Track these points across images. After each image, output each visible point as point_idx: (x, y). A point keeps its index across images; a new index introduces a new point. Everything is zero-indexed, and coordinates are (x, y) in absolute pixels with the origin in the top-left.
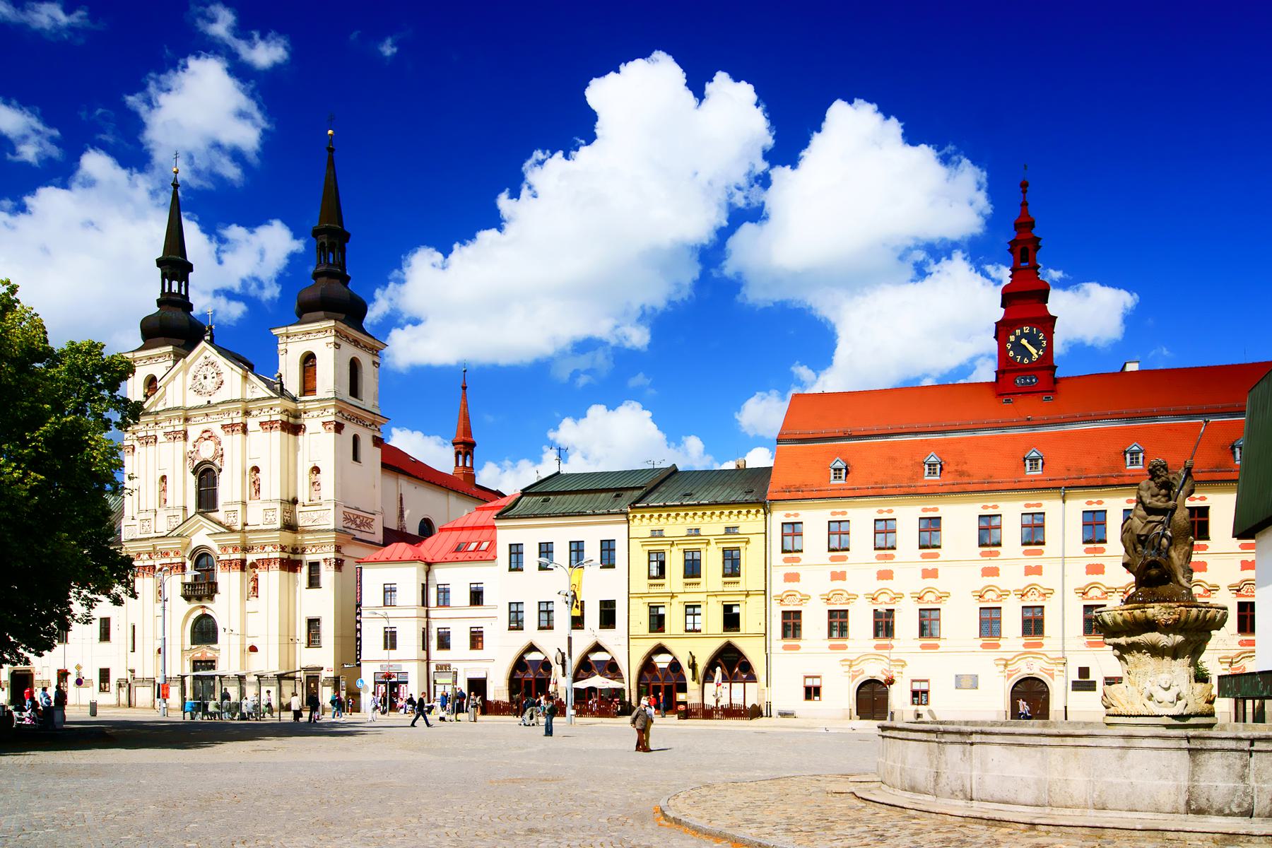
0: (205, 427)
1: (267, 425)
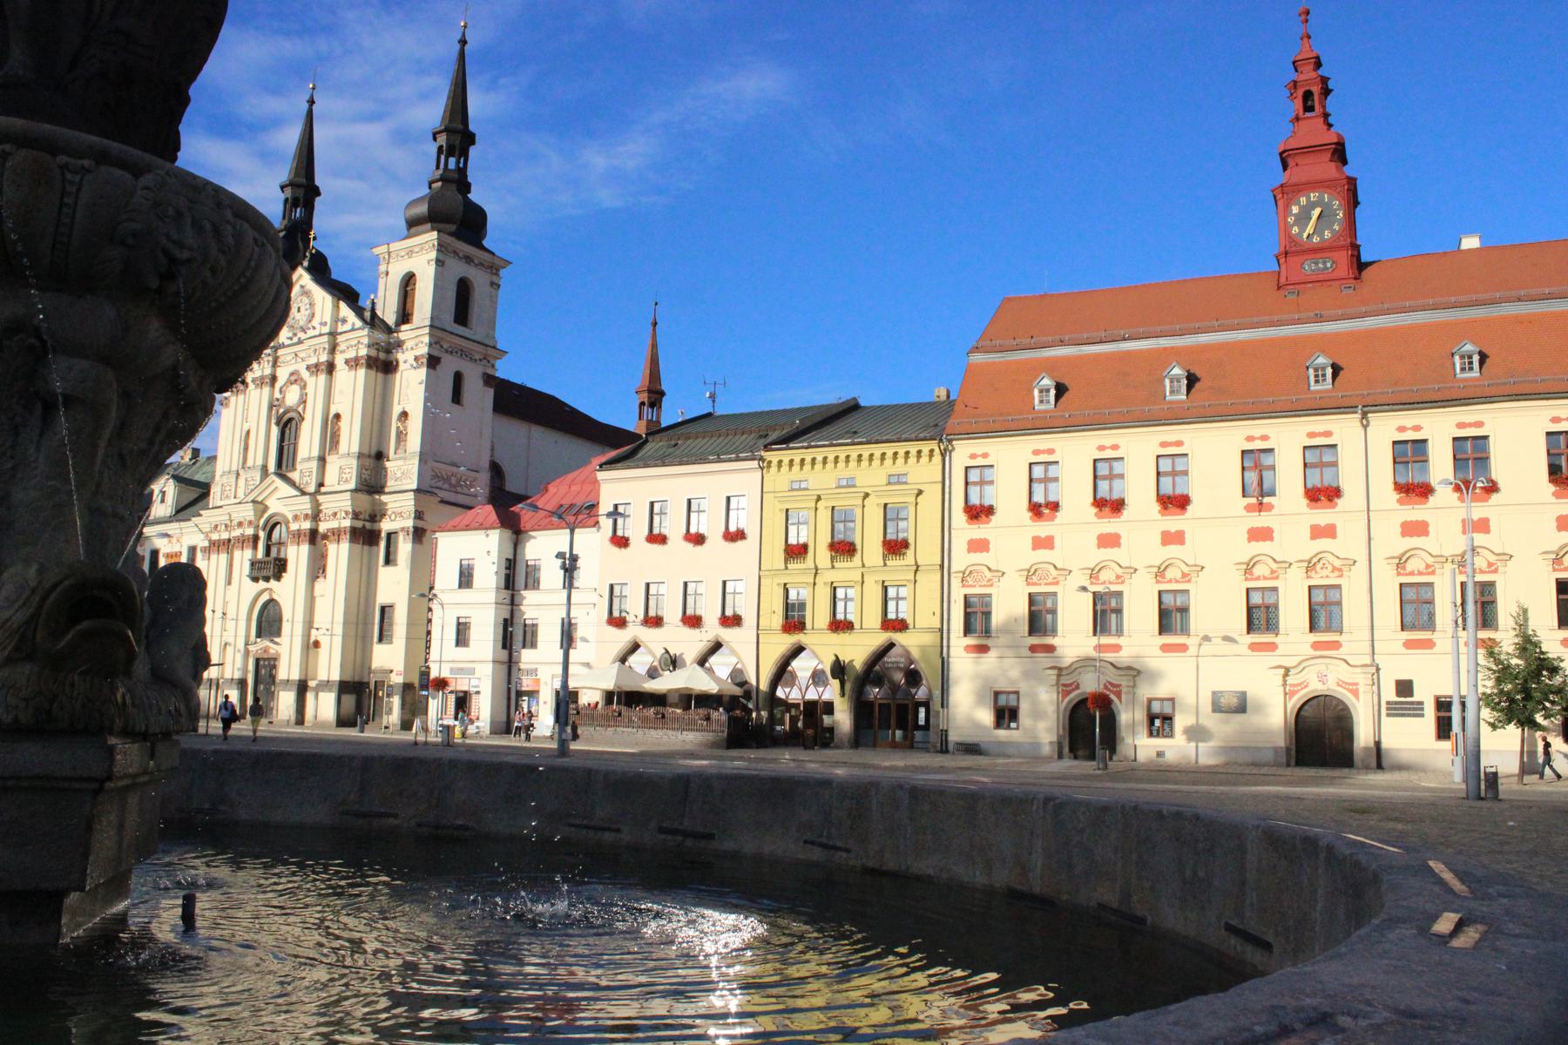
1: (353, 363)
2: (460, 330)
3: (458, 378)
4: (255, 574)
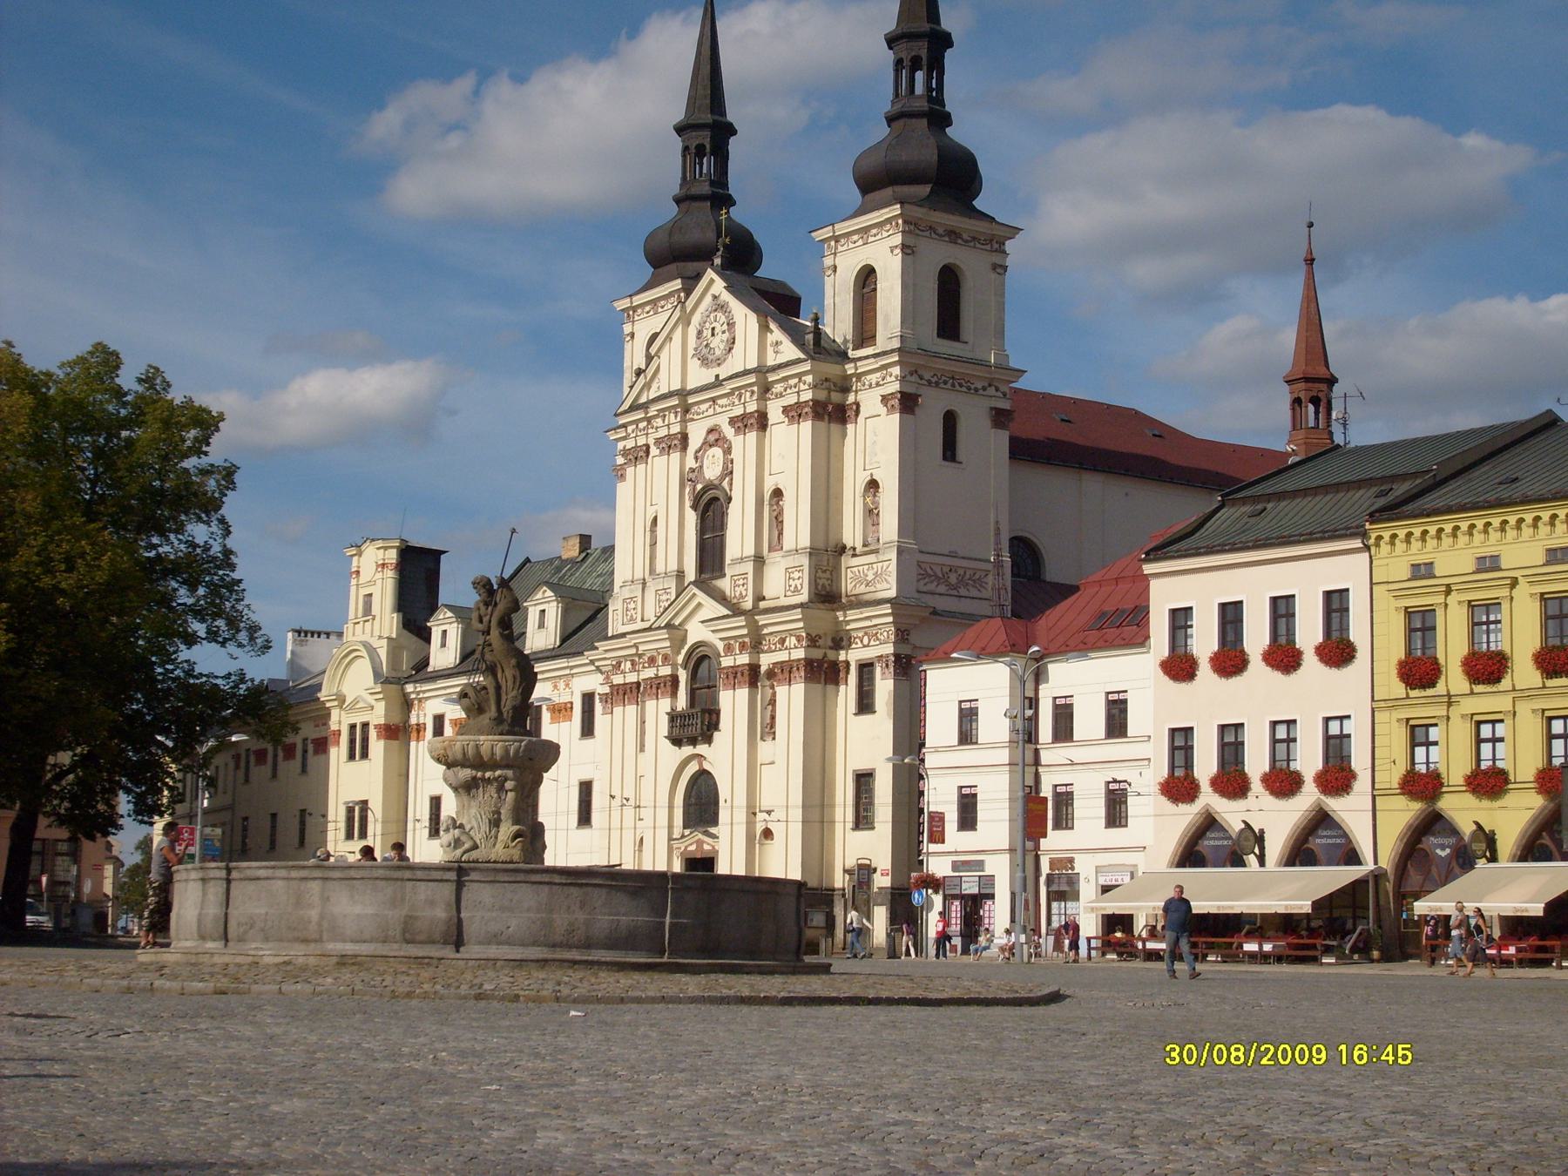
0: (709, 423)
2: (946, 347)
3: (950, 420)
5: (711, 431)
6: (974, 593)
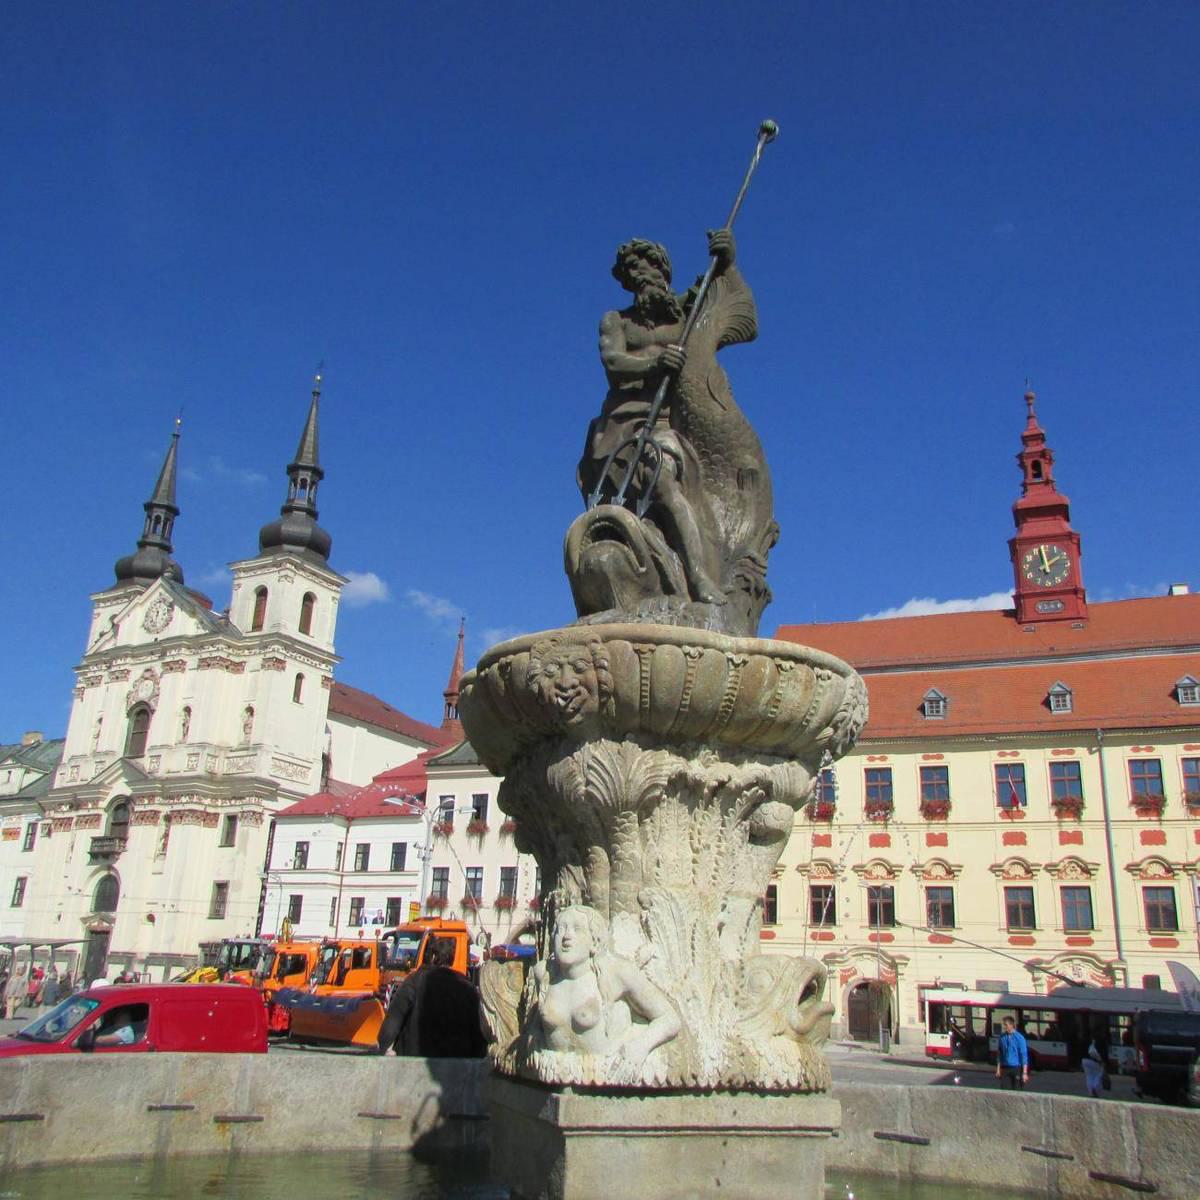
0: (148, 666)
2: (302, 637)
4: (96, 849)
5: (147, 670)
6: (300, 780)
